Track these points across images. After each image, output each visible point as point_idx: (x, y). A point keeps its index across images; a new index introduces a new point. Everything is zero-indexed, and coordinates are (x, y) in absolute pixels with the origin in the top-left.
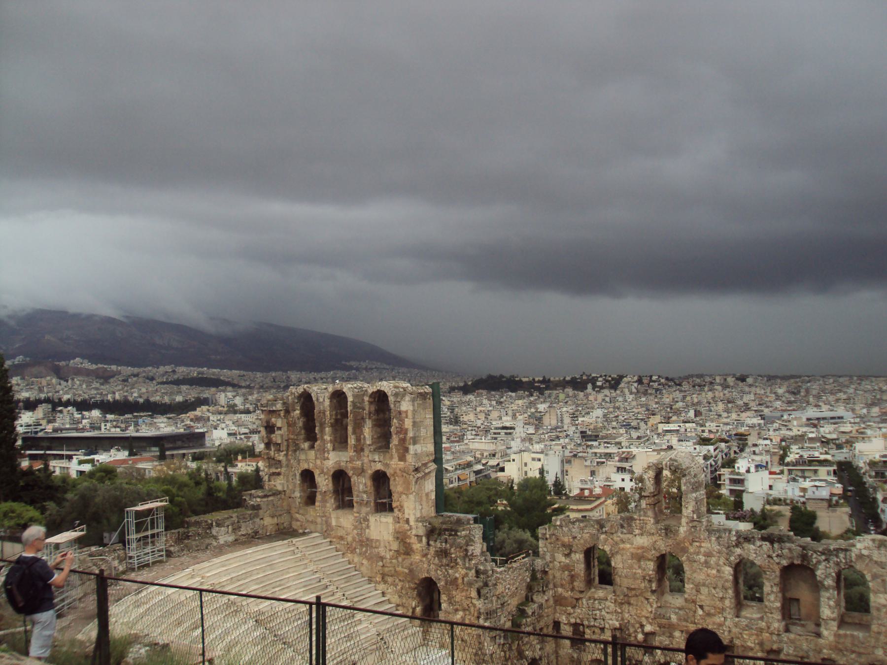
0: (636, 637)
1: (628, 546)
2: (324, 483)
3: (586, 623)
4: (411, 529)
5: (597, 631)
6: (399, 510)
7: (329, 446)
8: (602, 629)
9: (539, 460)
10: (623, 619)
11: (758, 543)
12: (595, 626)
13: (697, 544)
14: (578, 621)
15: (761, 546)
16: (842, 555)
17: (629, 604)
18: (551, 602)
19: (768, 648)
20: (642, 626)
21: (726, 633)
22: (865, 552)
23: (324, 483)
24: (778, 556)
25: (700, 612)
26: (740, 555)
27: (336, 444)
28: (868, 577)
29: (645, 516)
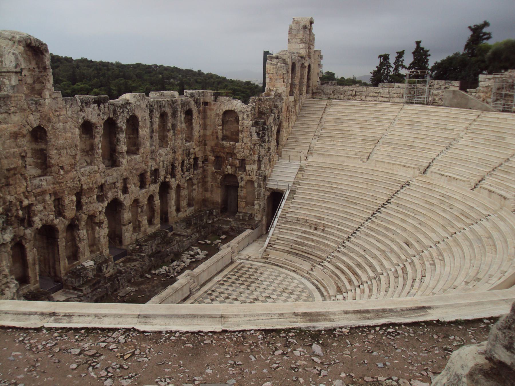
0: (17, 217)
1: (5, 126)
10: (4, 203)
11: (92, 106)
13: (58, 113)
15: (93, 109)
16: (128, 107)
19: (100, 184)
20: (21, 202)
21: (78, 183)
22: (138, 103)
24: (103, 113)
25: (62, 172)
26: (84, 117)
28: (140, 119)
29: (18, 92)
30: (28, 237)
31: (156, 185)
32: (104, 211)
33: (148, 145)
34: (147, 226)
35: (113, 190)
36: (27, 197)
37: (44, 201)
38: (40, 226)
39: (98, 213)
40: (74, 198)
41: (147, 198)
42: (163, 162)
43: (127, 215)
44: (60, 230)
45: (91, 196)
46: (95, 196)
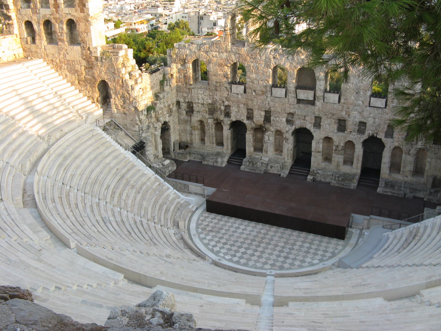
0: (220, 108)
2: (39, 29)
3: (194, 101)
4: (91, 52)
5: (200, 105)
6: (84, 43)
7: (39, 5)
8: (203, 104)
9: (186, 17)
10: (213, 98)
12: (199, 103)
14: (190, 101)
17: (217, 90)
18: (175, 91)
20: (223, 102)
21: (267, 104)
23: (39, 29)
25: (254, 94)
27: (43, 4)
30: (225, 122)
31: (359, 136)
32: (291, 132)
33: (353, 98)
34: (342, 164)
35: (302, 121)
36: (228, 101)
37: (238, 107)
38: (234, 120)
39: (285, 132)
40: (263, 114)
41: (344, 141)
42: (374, 118)
43: (317, 145)
44: (247, 128)
45: (278, 117)
46: (284, 119)
